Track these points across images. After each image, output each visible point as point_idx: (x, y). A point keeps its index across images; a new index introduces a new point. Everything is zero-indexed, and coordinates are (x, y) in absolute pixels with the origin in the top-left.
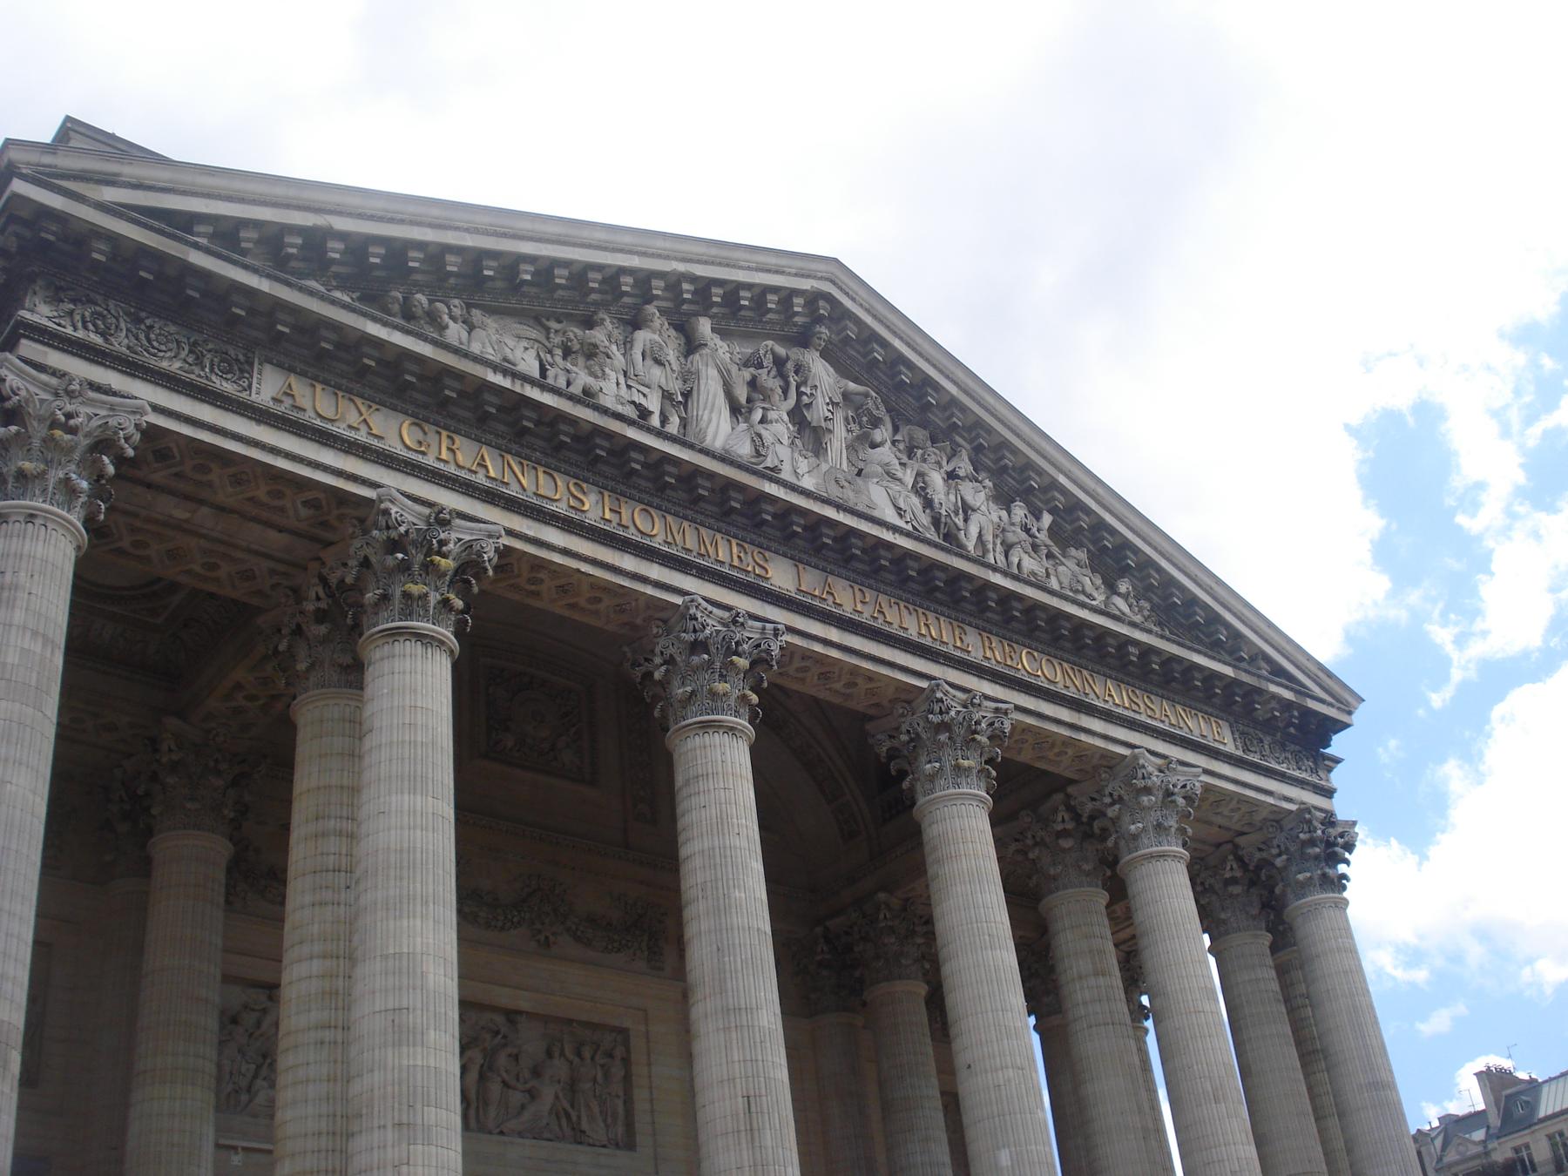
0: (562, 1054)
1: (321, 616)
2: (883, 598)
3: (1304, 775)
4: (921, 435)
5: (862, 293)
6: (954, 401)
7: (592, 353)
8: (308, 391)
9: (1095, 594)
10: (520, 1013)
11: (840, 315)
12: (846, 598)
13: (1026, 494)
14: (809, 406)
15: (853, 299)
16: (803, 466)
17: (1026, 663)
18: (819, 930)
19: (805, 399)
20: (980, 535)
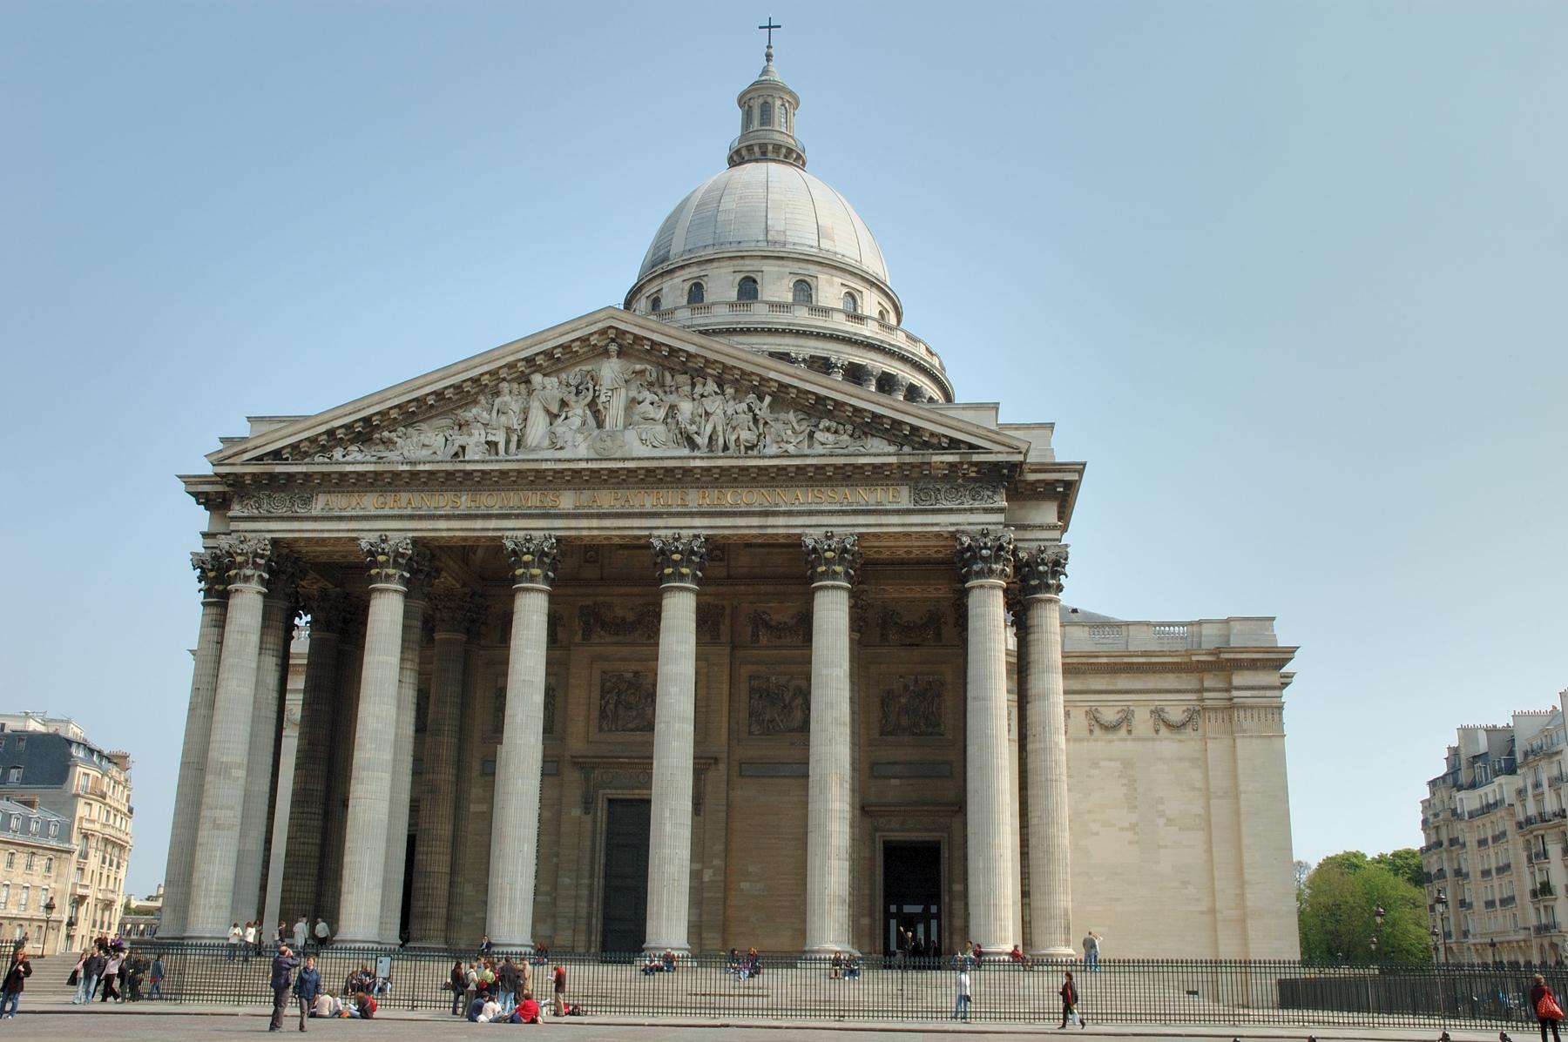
2: (630, 493)
3: (976, 505)
4: (681, 379)
7: (467, 423)
11: (621, 333)
12: (607, 499)
13: (754, 389)
16: (580, 438)
17: (729, 498)
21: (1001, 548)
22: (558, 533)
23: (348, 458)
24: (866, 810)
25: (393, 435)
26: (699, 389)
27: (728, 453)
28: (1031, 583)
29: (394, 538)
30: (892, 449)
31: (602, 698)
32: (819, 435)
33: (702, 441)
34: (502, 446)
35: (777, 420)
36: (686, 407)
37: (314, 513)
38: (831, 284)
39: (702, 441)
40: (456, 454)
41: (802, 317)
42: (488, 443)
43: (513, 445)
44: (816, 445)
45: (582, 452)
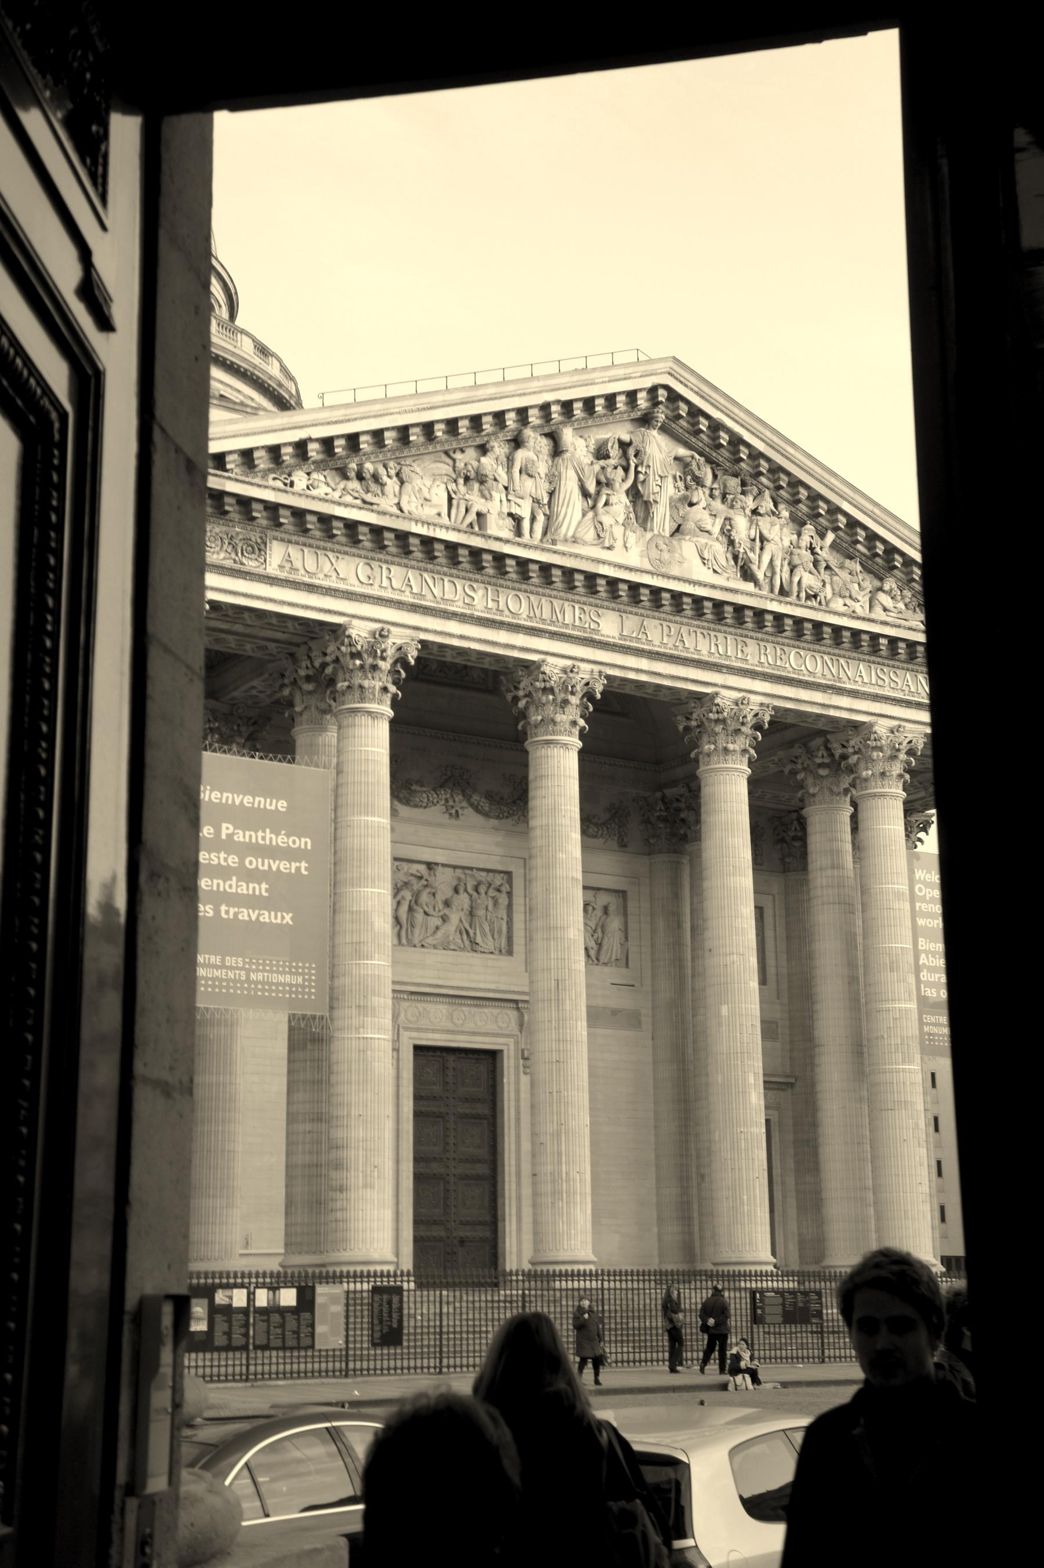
0: (466, 890)
1: (308, 679)
2: (684, 630)
4: (733, 483)
5: (693, 379)
6: (761, 455)
7: (481, 479)
8: (299, 555)
9: (860, 598)
10: (437, 864)
11: (674, 397)
12: (657, 633)
15: (686, 386)
18: (659, 795)
19: (641, 477)
20: (771, 560)
22: (611, 672)
23: (314, 493)
27: (793, 598)
29: (397, 638)
31: (395, 896)
36: (742, 526)
39: (760, 575)
40: (471, 525)
42: (510, 515)
44: (878, 609)
45: (634, 558)
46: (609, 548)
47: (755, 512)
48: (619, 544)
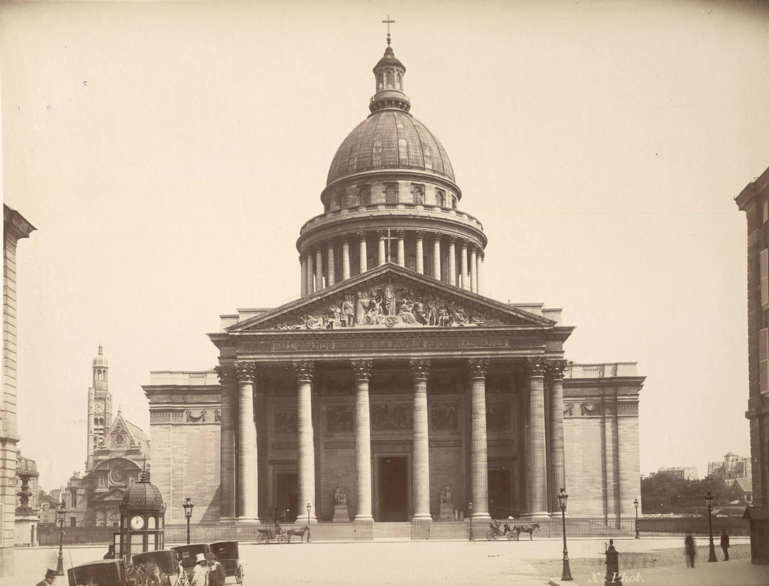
7: (333, 313)
14: (385, 301)
20: (432, 314)
21: (543, 363)
24: (490, 460)
25: (302, 318)
26: (425, 298)
28: (553, 371)
30: (502, 324)
32: (473, 318)
33: (428, 320)
34: (347, 322)
35: (457, 312)
37: (272, 351)
38: (431, 188)
39: (428, 320)
40: (328, 327)
41: (420, 211)
43: (351, 323)
46: (372, 324)
47: (426, 300)
48: (375, 321)
